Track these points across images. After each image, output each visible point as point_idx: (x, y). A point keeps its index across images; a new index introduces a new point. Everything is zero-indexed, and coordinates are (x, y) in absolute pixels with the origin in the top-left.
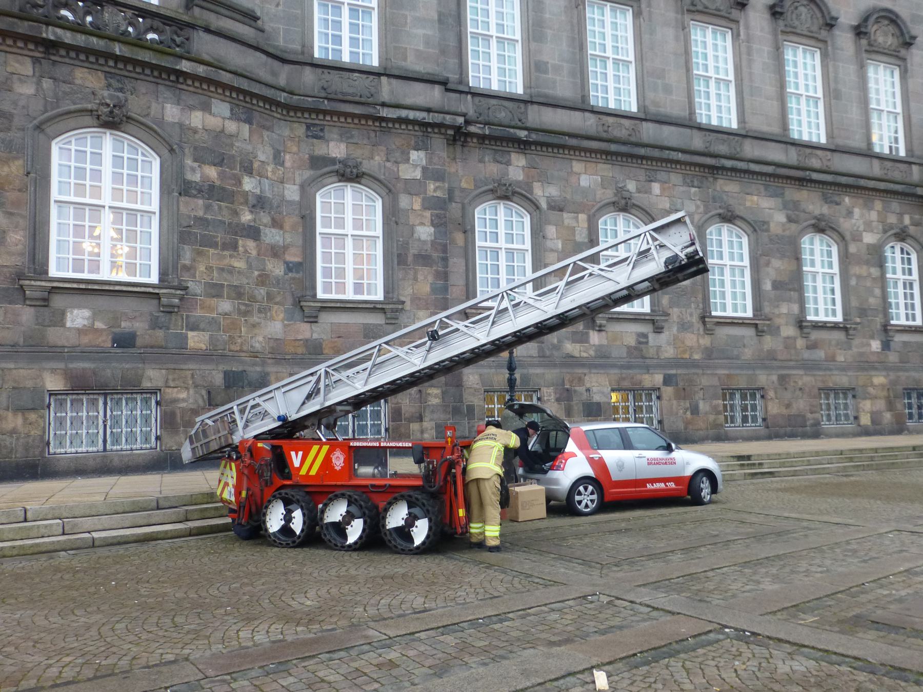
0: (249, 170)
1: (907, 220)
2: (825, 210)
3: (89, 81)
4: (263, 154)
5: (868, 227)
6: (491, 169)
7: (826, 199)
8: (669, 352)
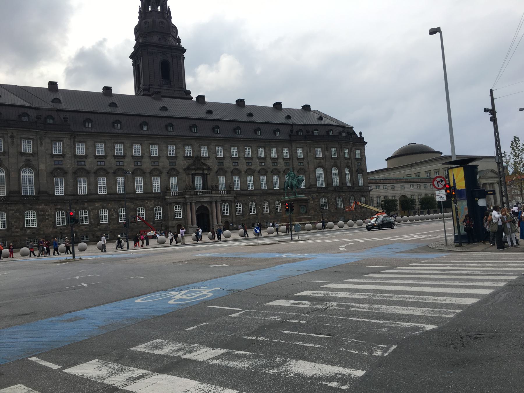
0: (47, 211)
2: (142, 203)
3: (28, 205)
5: (151, 205)
6: (82, 206)
8: (111, 228)
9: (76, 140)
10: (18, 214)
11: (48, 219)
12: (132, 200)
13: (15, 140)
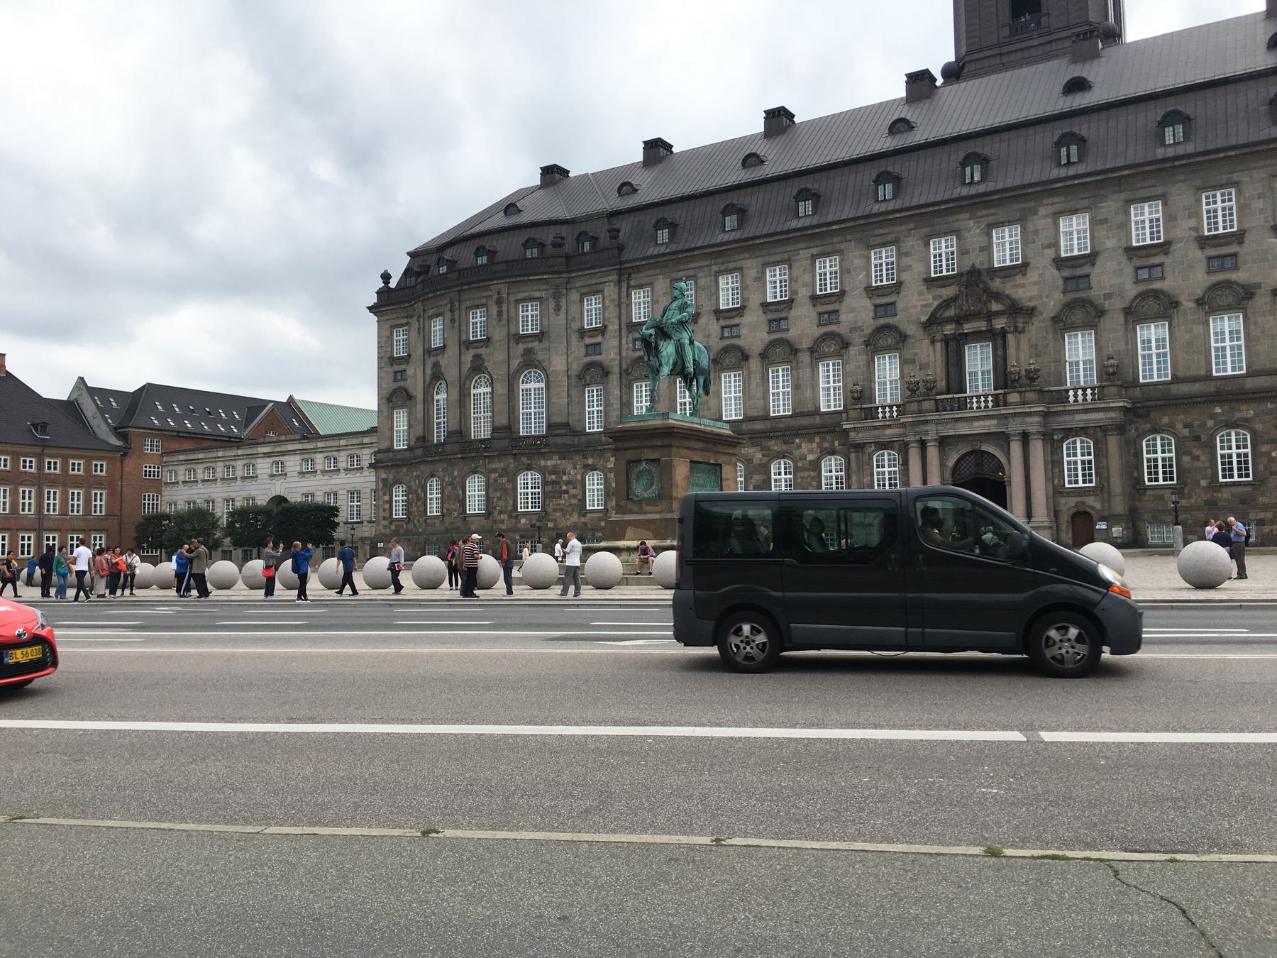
1: (836, 443)
2: (784, 447)
3: (524, 460)
4: (569, 467)
5: (811, 452)
7: (785, 443)
9: (632, 283)
10: (504, 480)
11: (566, 492)
12: (757, 438)
13: (504, 308)
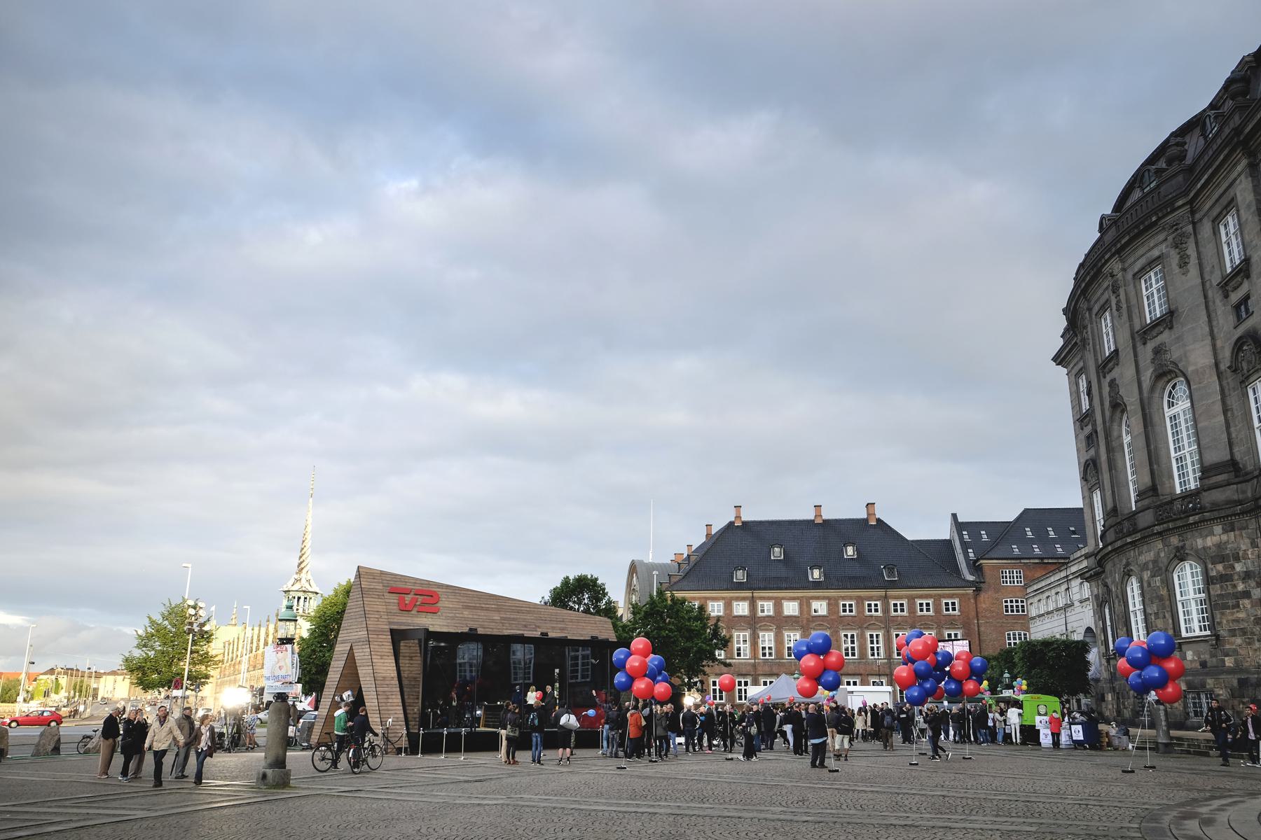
0: (1237, 559)
11: (1246, 594)
